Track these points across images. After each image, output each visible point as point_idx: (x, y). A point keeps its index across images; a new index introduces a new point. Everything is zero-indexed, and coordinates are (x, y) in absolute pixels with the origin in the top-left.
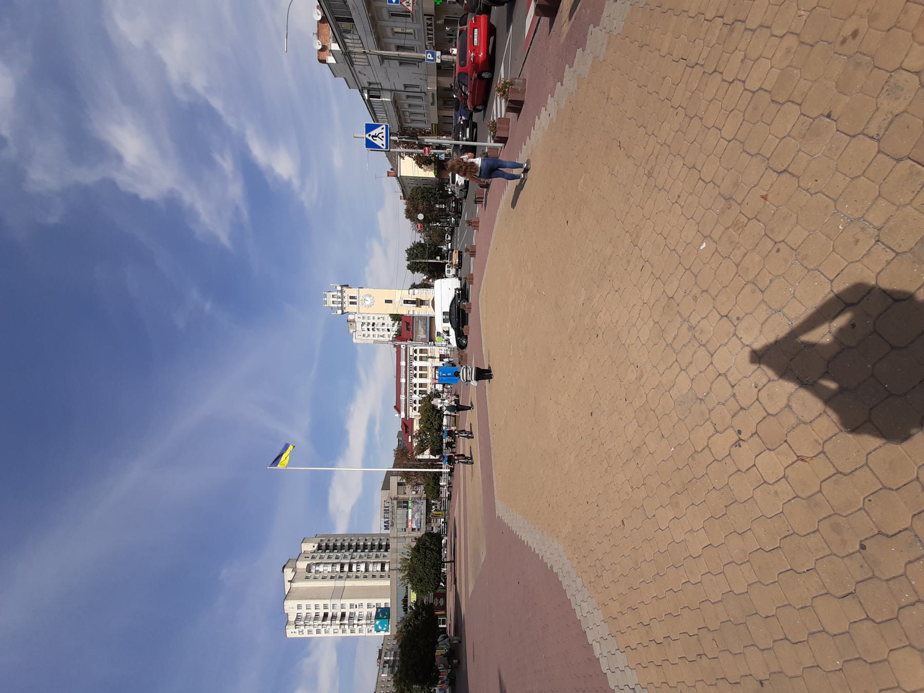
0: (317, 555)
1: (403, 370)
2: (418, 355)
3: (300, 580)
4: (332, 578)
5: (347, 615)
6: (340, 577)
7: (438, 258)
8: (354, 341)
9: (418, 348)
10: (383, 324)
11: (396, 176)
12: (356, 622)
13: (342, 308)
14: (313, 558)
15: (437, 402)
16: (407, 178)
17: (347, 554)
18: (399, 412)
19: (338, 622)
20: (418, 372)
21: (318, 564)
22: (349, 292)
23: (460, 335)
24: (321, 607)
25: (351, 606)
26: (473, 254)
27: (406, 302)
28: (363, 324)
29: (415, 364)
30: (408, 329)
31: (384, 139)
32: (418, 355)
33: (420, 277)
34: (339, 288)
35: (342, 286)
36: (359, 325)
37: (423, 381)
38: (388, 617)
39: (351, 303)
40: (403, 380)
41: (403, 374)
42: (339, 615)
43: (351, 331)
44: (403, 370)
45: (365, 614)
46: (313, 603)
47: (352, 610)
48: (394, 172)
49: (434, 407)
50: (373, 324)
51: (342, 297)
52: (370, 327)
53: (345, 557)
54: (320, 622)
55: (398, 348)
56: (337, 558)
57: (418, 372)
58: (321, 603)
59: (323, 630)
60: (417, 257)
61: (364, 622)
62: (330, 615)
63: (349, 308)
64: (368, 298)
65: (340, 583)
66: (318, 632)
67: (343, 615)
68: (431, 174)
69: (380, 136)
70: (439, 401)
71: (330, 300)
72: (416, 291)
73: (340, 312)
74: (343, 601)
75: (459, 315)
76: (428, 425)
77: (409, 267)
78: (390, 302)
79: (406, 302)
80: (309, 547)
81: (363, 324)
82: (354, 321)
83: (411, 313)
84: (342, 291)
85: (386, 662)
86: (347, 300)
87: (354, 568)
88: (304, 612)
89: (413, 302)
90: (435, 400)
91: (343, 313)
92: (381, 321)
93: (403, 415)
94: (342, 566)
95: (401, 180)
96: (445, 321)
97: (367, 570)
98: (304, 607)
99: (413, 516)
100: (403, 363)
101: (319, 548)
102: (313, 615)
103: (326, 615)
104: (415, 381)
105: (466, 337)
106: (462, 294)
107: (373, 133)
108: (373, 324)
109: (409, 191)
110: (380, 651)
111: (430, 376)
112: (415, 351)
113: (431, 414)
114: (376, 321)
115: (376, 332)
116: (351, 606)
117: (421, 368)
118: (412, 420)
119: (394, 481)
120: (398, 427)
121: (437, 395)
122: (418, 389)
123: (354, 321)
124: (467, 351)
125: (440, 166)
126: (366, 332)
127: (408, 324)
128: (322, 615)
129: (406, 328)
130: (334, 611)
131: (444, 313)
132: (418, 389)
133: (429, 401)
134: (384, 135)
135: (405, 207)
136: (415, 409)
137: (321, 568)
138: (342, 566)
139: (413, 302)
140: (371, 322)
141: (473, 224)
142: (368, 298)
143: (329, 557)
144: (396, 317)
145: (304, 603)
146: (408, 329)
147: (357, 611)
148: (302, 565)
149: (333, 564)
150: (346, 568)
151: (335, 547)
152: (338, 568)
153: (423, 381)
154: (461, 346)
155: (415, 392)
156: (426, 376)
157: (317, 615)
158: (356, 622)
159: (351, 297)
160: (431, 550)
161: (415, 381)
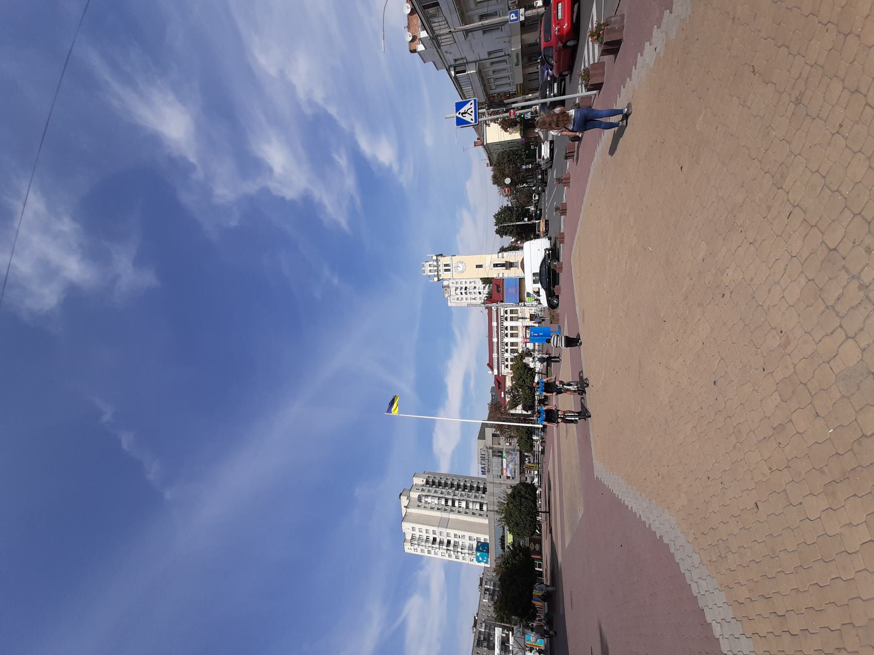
0: (427, 488)
1: (495, 330)
2: (509, 315)
3: (413, 507)
4: (438, 509)
5: (452, 542)
6: (445, 510)
7: (526, 219)
8: (449, 304)
9: (509, 309)
10: (475, 288)
11: (483, 144)
12: (459, 550)
13: (438, 276)
14: (422, 490)
15: (528, 360)
16: (492, 144)
17: (450, 491)
18: (492, 369)
19: (444, 547)
20: (509, 332)
21: (427, 496)
22: (443, 261)
23: (551, 295)
24: (431, 532)
25: (455, 536)
26: (563, 212)
27: (496, 265)
28: (456, 289)
29: (506, 324)
30: (498, 291)
31: (473, 114)
32: (509, 315)
33: (508, 240)
34: (435, 258)
37: (514, 340)
38: (488, 551)
39: (446, 270)
40: (495, 340)
41: (495, 334)
42: (446, 541)
43: (446, 295)
44: (495, 330)
45: (467, 545)
46: (424, 527)
47: (456, 540)
48: (481, 141)
49: (526, 366)
50: (466, 288)
51: (438, 266)
52: (463, 291)
53: (448, 493)
54: (430, 545)
55: (490, 309)
56: (442, 493)
57: (509, 332)
58: (431, 529)
59: (433, 552)
60: (505, 221)
61: (466, 551)
62: (438, 540)
63: (444, 275)
64: (460, 265)
65: (445, 515)
66: (429, 552)
67: (449, 542)
68: (517, 136)
69: (469, 112)
70: (531, 359)
71: (428, 269)
72: (505, 254)
73: (436, 279)
74: (448, 531)
75: (549, 276)
76: (520, 382)
77: (498, 232)
78: (481, 266)
79: (496, 265)
80: (419, 481)
81: (456, 289)
82: (448, 287)
83: (501, 276)
84: (437, 260)
85: (486, 590)
87: (457, 504)
88: (417, 534)
89: (502, 265)
90: (527, 358)
91: (439, 280)
92: (473, 285)
93: (496, 372)
94: (446, 501)
95: (488, 148)
96: (535, 282)
97: (467, 507)
98: (417, 530)
99: (507, 466)
100: (494, 324)
101: (427, 483)
102: (425, 538)
103: (435, 539)
104: (506, 340)
105: (558, 297)
106: (553, 254)
107: (462, 111)
108: (466, 288)
109: (495, 157)
110: (481, 579)
111: (521, 334)
112: (506, 312)
113: (523, 372)
114: (468, 285)
115: (469, 296)
116: (455, 536)
117: (512, 328)
118: (505, 376)
119: (489, 432)
120: (492, 383)
121: (528, 353)
122: (509, 348)
123: (448, 287)
124: (558, 310)
125: (527, 125)
126: (460, 296)
127: (498, 286)
128: (431, 539)
129: (495, 290)
130: (442, 537)
131: (534, 274)
132: (509, 348)
133: (521, 360)
134: (473, 109)
135: (492, 173)
136: (507, 366)
137: (429, 500)
138: (446, 501)
139: (502, 265)
140: (464, 286)
141: (564, 181)
142: (460, 265)
143: (435, 492)
144: (486, 281)
145: (417, 526)
146: (498, 291)
147: (460, 541)
148: (414, 495)
149: (439, 498)
150: (450, 503)
151: (440, 484)
152: (443, 502)
153: (514, 340)
154: (552, 306)
155: (507, 351)
156: (516, 335)
157: (427, 538)
158: (459, 550)
159: (446, 265)
160: (527, 498)
161: (506, 340)
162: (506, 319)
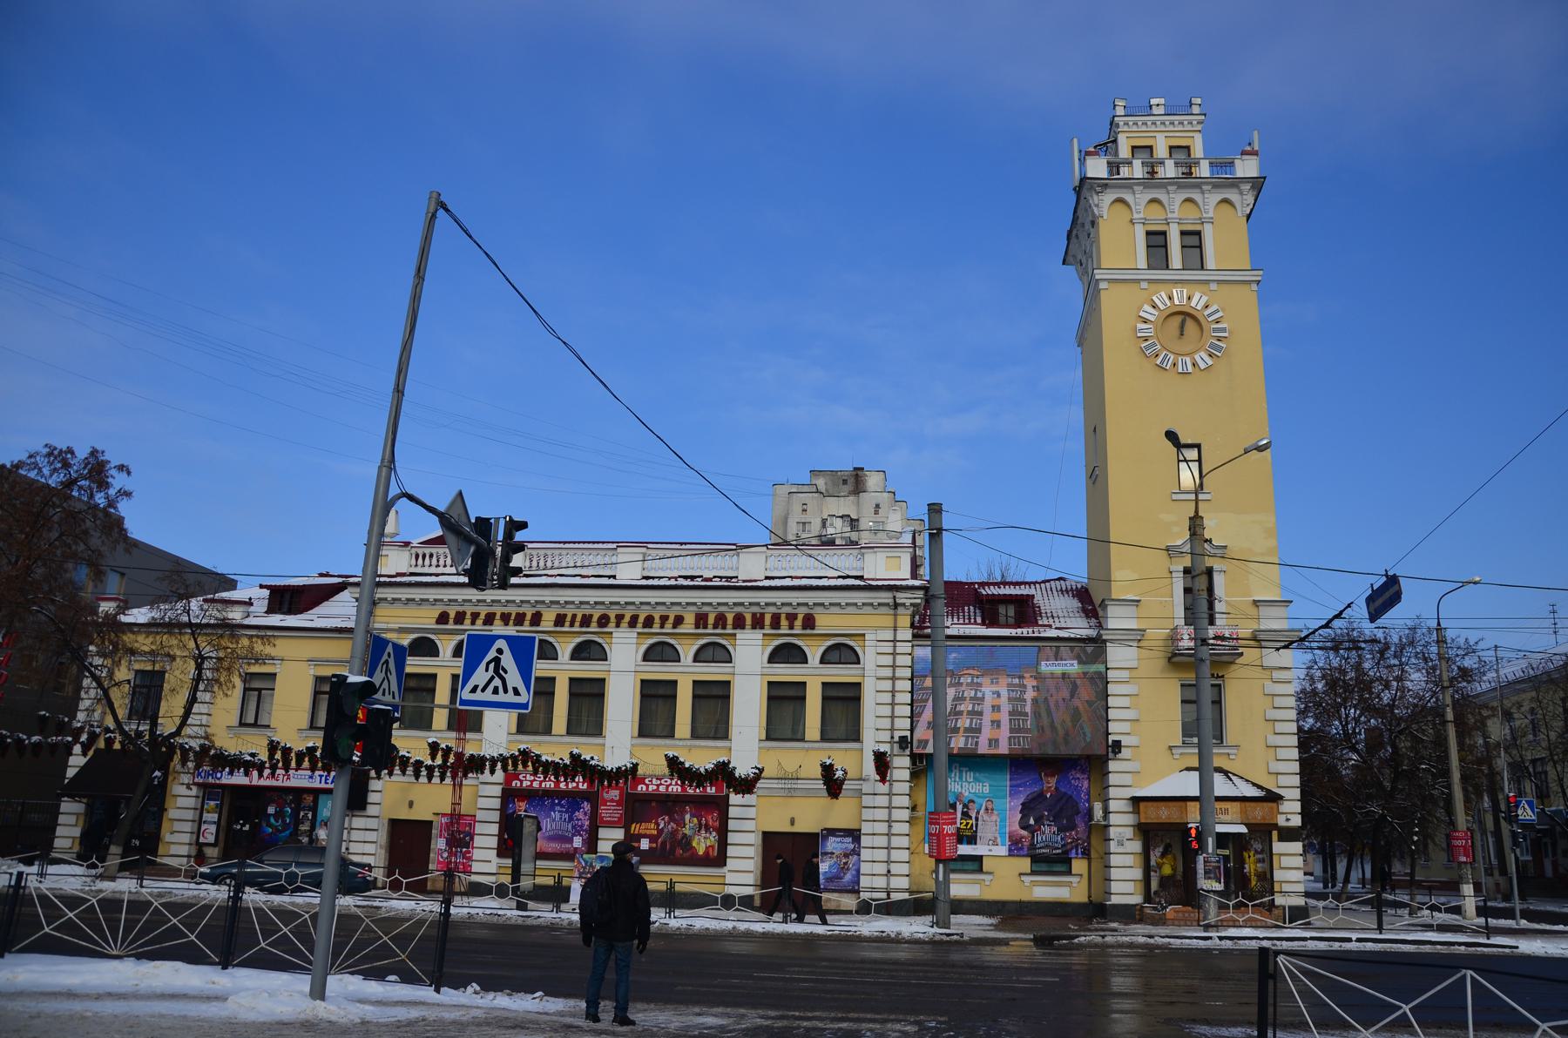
2: (814, 676)
20: (686, 673)
32: (814, 676)
34: (1247, 168)
35: (1258, 184)
36: (845, 506)
37: (622, 706)
39: (1157, 242)
44: (709, 566)
57: (686, 673)
73: (1097, 168)
84: (1225, 180)
86: (1175, 213)
91: (1084, 186)
112: (842, 652)
153: (622, 706)
159: (1193, 239)
162: (787, 653)
